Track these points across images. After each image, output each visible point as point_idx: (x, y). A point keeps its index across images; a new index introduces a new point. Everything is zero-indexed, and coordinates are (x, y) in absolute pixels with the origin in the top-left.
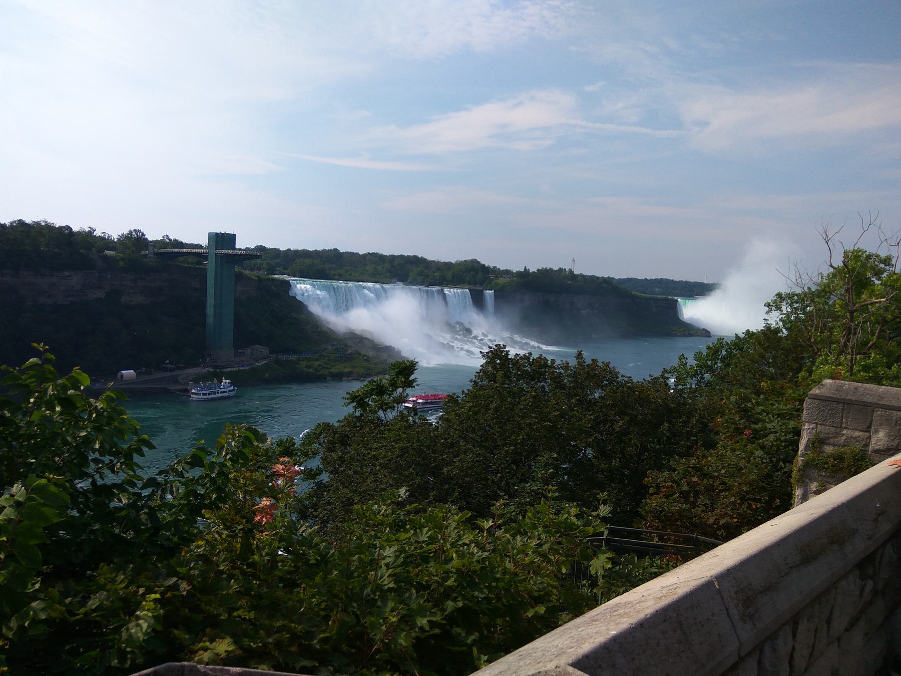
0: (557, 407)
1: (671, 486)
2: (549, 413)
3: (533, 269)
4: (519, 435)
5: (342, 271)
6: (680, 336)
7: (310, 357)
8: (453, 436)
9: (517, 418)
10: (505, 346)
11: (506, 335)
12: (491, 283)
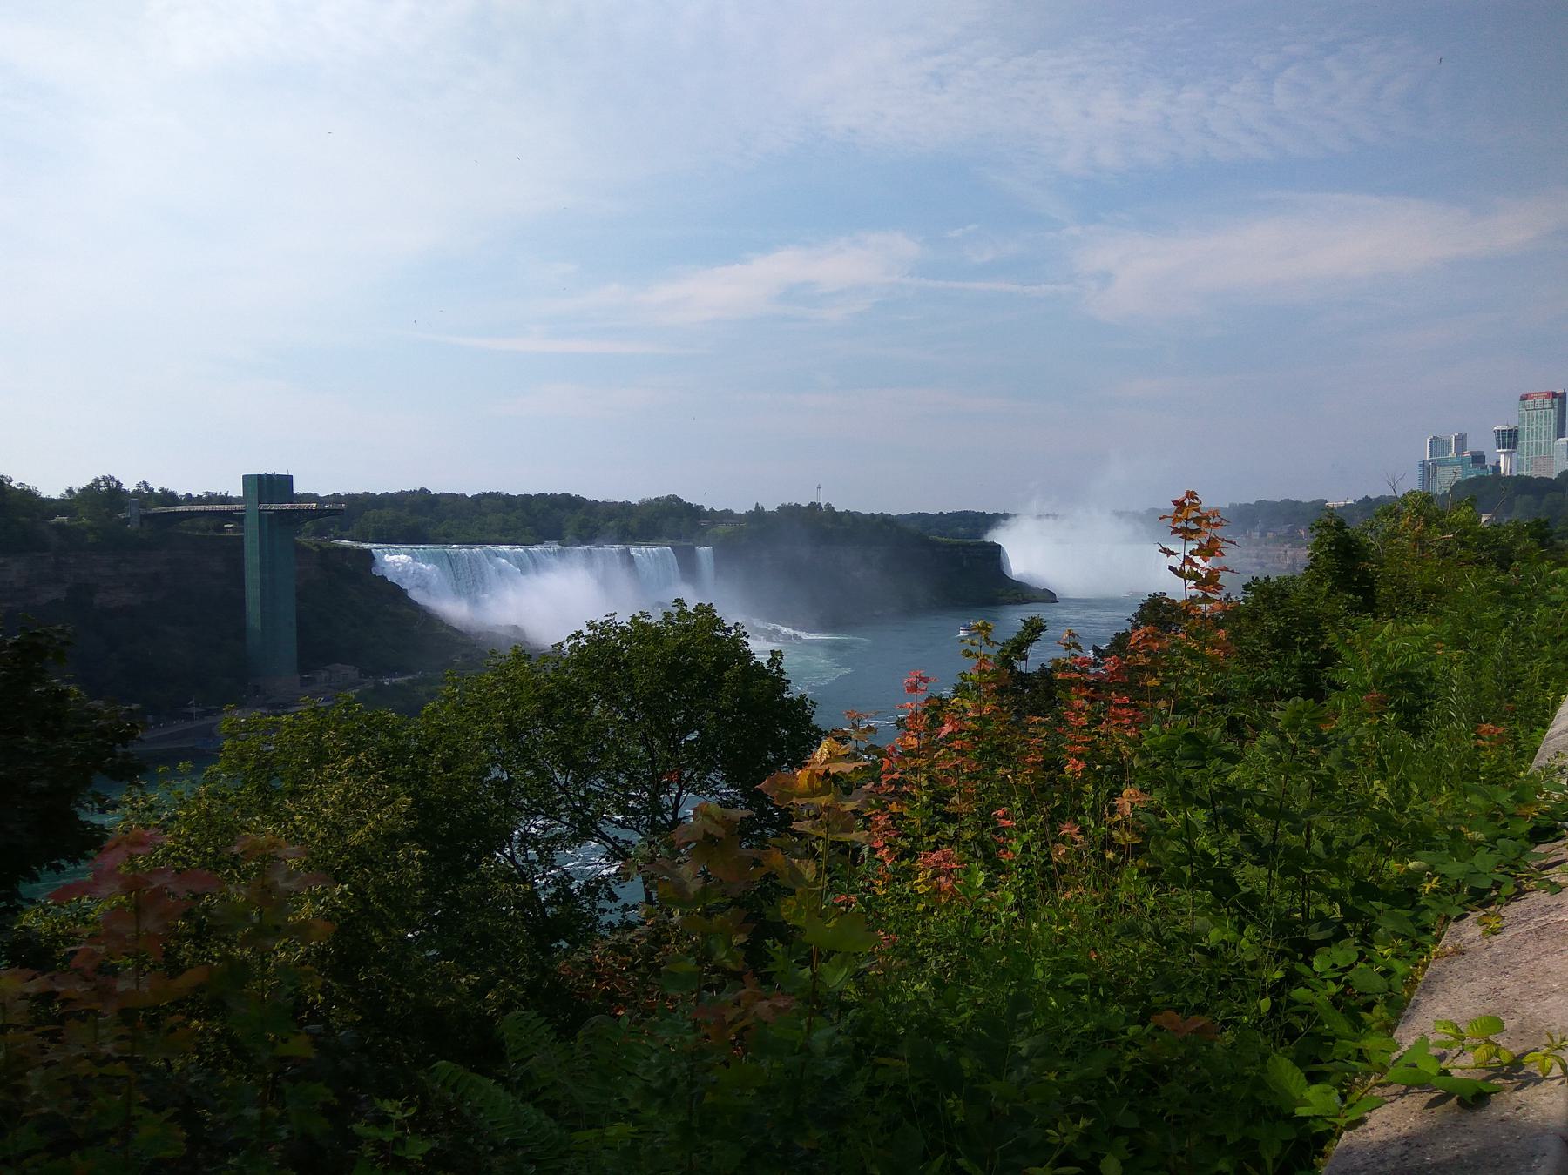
3: (770, 507)
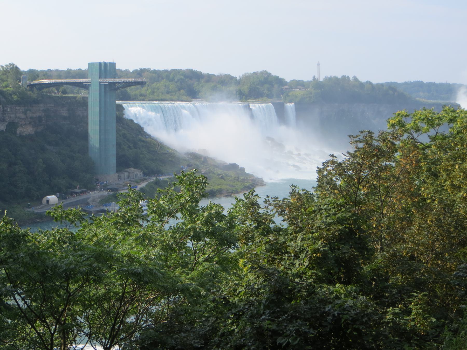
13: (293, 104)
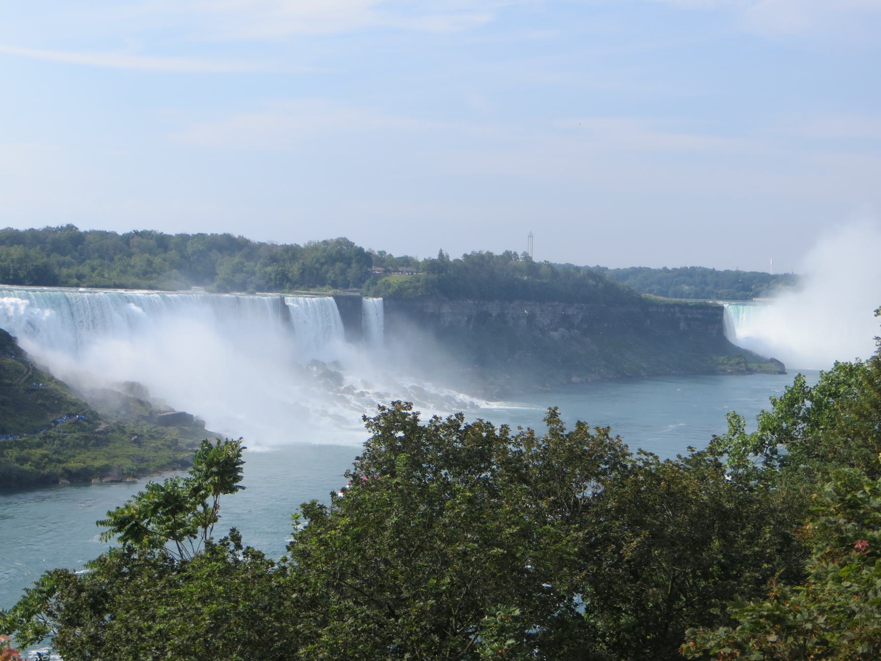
0: (514, 519)
1: (732, 655)
2: (500, 530)
3: (455, 254)
4: (443, 576)
5: (85, 269)
6: (731, 374)
7: (24, 441)
8: (316, 584)
9: (439, 543)
10: (409, 406)
11: (408, 383)
12: (376, 284)
13: (381, 299)
